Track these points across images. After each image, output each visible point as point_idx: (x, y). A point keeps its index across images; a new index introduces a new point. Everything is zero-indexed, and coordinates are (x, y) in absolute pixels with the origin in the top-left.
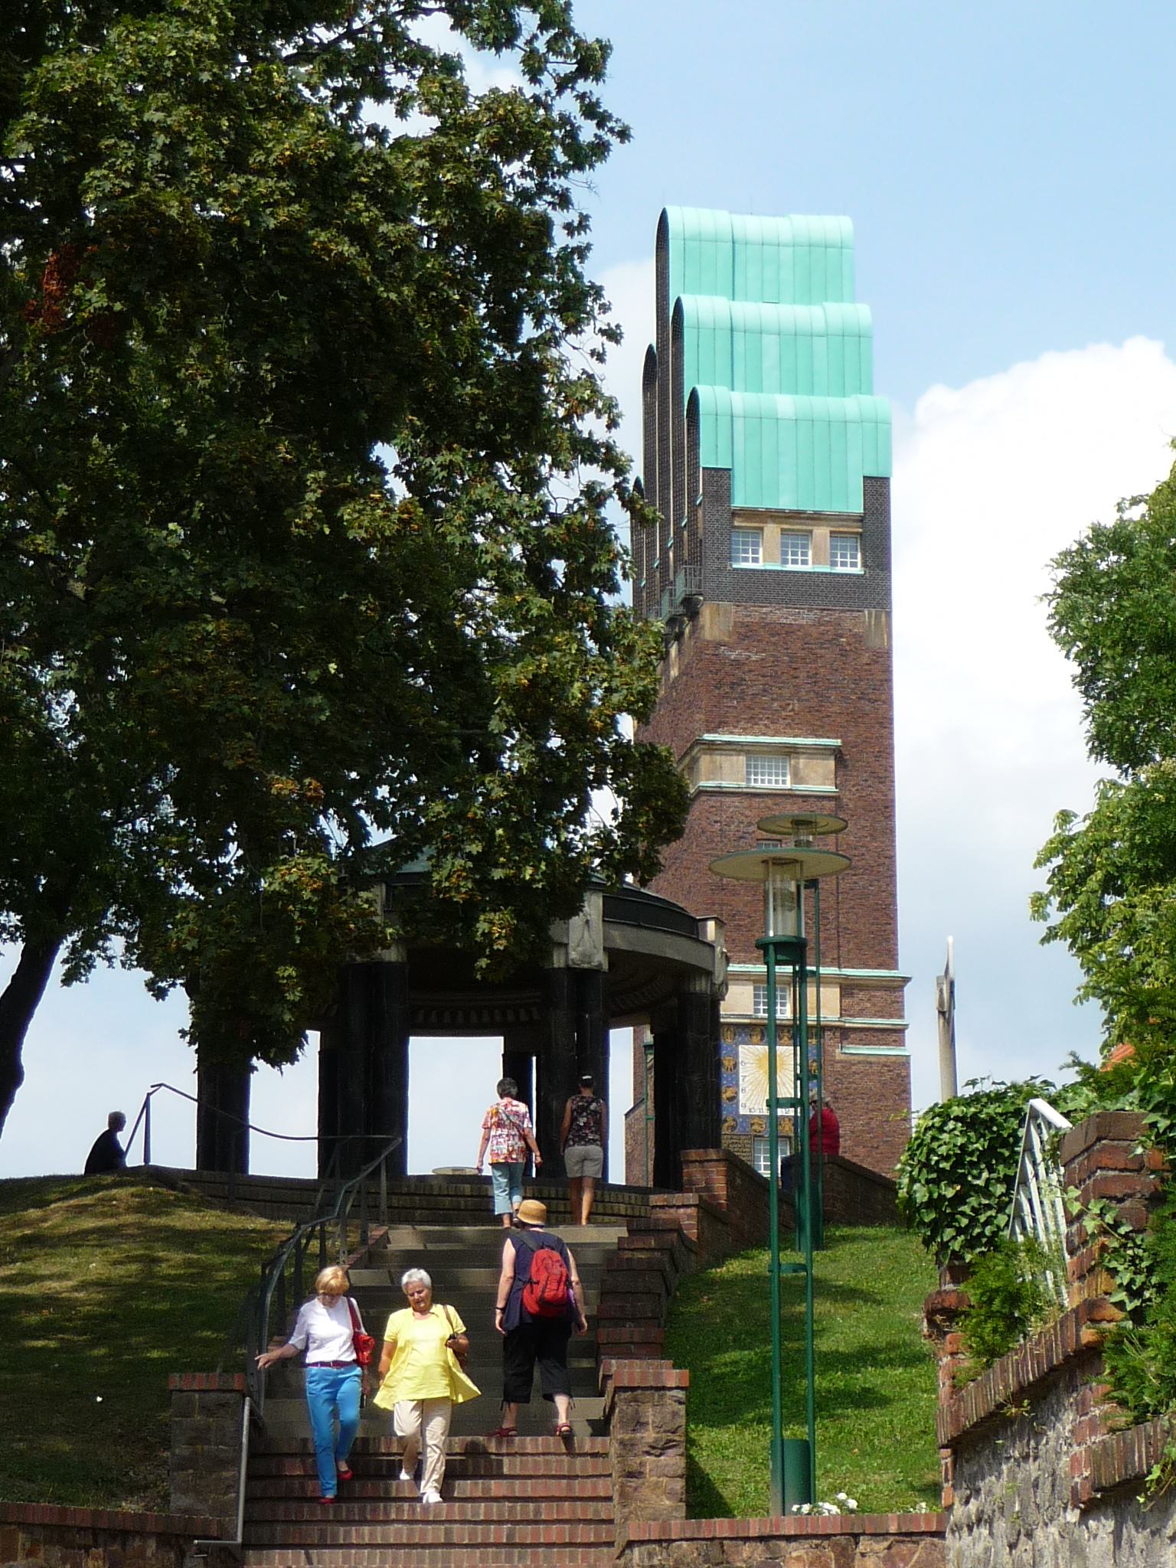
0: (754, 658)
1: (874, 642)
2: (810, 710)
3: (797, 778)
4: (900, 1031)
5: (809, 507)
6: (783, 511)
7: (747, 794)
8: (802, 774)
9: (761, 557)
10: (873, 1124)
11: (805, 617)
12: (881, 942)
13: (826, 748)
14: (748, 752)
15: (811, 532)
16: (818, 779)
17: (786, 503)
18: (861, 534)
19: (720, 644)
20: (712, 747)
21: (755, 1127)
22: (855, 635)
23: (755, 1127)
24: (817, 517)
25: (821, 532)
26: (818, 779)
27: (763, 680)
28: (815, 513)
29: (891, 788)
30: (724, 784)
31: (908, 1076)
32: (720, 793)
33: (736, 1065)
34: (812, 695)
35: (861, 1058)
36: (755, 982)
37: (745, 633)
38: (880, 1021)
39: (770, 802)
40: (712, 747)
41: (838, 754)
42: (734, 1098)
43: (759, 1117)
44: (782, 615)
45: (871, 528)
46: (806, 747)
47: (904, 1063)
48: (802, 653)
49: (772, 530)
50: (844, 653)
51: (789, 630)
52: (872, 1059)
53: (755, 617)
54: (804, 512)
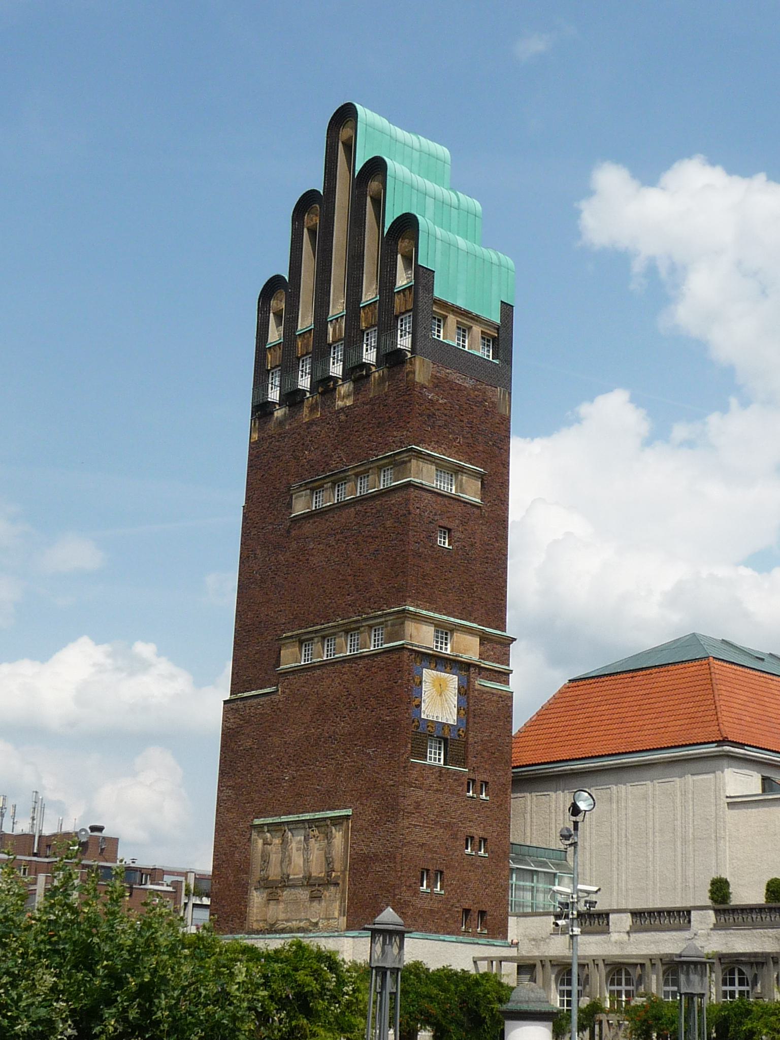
0: (440, 401)
1: (502, 410)
2: (469, 445)
3: (460, 487)
4: (507, 674)
5: (475, 311)
6: (458, 308)
7: (435, 492)
8: (465, 486)
9: (447, 335)
10: (493, 737)
11: (469, 383)
12: (495, 610)
13: (479, 473)
14: (437, 465)
15: (470, 328)
16: (472, 494)
17: (460, 303)
18: (494, 339)
19: (423, 386)
20: (419, 455)
21: (429, 729)
22: (493, 402)
23: (429, 729)
24: (476, 319)
25: (477, 329)
26: (472, 494)
27: (444, 418)
28: (477, 316)
29: (507, 509)
30: (424, 482)
31: (512, 706)
32: (421, 488)
33: (421, 683)
34: (469, 435)
35: (488, 689)
36: (436, 626)
37: (438, 383)
38: (497, 665)
39: (446, 501)
40: (419, 455)
41: (482, 477)
42: (419, 706)
43: (432, 721)
44: (456, 378)
45: (500, 338)
46: (469, 469)
47: (509, 697)
48: (466, 406)
49: (452, 319)
50: (487, 412)
51: (460, 389)
52: (494, 691)
53: (442, 375)
54: (471, 313)
